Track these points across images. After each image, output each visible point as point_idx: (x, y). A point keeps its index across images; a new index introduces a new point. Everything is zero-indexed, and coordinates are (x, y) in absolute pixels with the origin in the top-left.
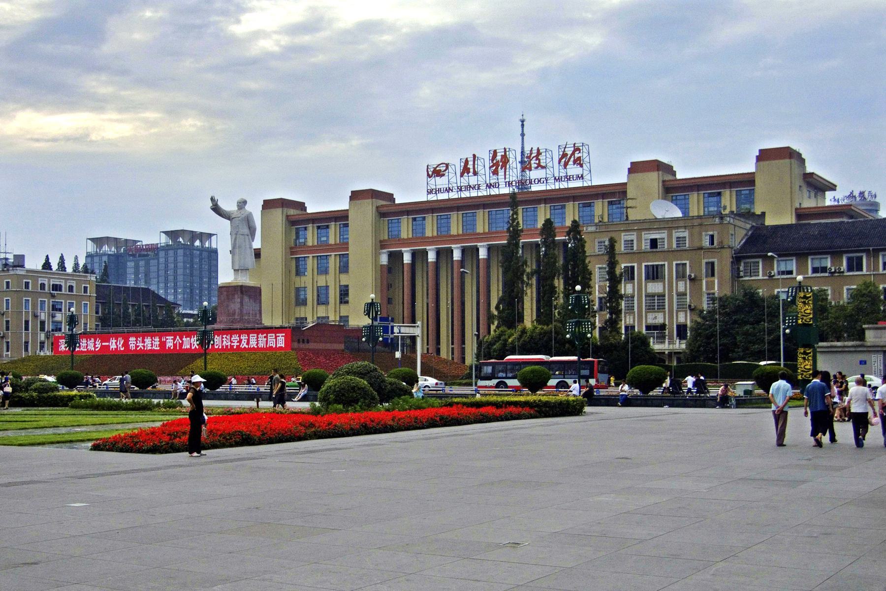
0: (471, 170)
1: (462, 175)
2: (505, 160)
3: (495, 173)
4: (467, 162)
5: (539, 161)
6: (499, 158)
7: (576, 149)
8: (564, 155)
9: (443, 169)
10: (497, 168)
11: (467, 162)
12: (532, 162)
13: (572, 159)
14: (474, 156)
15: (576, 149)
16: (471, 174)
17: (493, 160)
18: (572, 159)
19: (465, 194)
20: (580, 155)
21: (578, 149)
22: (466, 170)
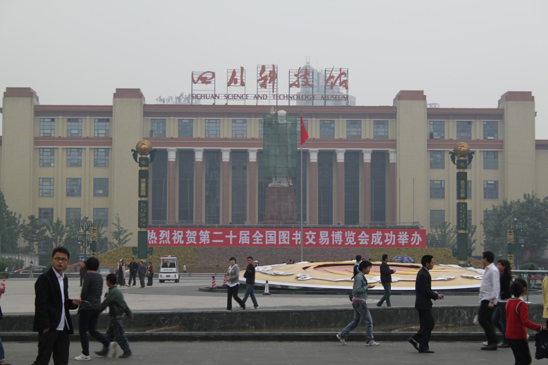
0: (239, 81)
1: (229, 84)
2: (273, 76)
3: (264, 86)
4: (234, 73)
5: (307, 79)
6: (267, 73)
7: (343, 73)
8: (331, 77)
9: (209, 76)
10: (265, 82)
11: (234, 73)
12: (300, 80)
13: (338, 81)
14: (242, 69)
15: (343, 73)
16: (239, 84)
17: (261, 74)
18: (338, 81)
19: (231, 103)
20: (345, 79)
21: (344, 73)
22: (232, 80)
